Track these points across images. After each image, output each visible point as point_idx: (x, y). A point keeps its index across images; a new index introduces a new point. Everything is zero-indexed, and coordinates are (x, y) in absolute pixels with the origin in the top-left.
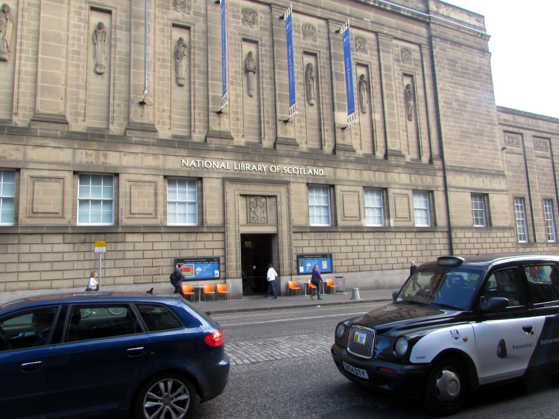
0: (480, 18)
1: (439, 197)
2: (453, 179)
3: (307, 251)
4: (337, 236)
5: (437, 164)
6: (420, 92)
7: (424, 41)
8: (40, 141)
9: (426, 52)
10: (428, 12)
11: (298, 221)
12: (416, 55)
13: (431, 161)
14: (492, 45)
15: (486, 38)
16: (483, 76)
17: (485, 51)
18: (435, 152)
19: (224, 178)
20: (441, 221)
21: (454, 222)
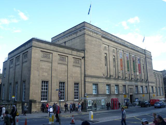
0: (150, 52)
1: (148, 87)
2: (150, 84)
3: (136, 98)
4: (138, 95)
5: (147, 81)
6: (145, 68)
7: (145, 58)
8: (112, 80)
9: (145, 59)
10: (145, 52)
11: (135, 92)
12: (144, 61)
13: (146, 81)
14: (152, 58)
15: (151, 56)
16: (151, 64)
17: (151, 59)
18: (147, 79)
19: (128, 85)
20: (148, 92)
21: (150, 92)
